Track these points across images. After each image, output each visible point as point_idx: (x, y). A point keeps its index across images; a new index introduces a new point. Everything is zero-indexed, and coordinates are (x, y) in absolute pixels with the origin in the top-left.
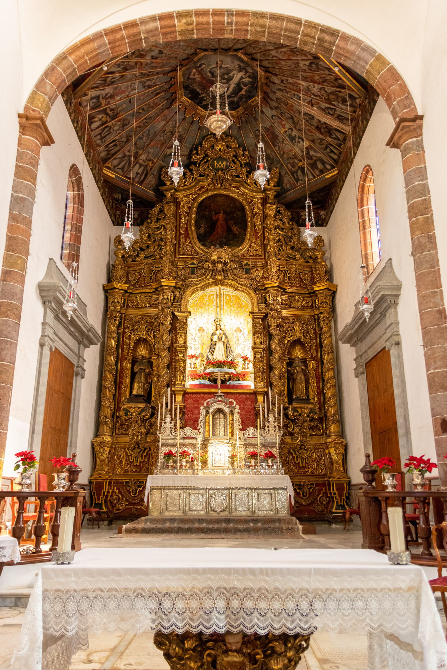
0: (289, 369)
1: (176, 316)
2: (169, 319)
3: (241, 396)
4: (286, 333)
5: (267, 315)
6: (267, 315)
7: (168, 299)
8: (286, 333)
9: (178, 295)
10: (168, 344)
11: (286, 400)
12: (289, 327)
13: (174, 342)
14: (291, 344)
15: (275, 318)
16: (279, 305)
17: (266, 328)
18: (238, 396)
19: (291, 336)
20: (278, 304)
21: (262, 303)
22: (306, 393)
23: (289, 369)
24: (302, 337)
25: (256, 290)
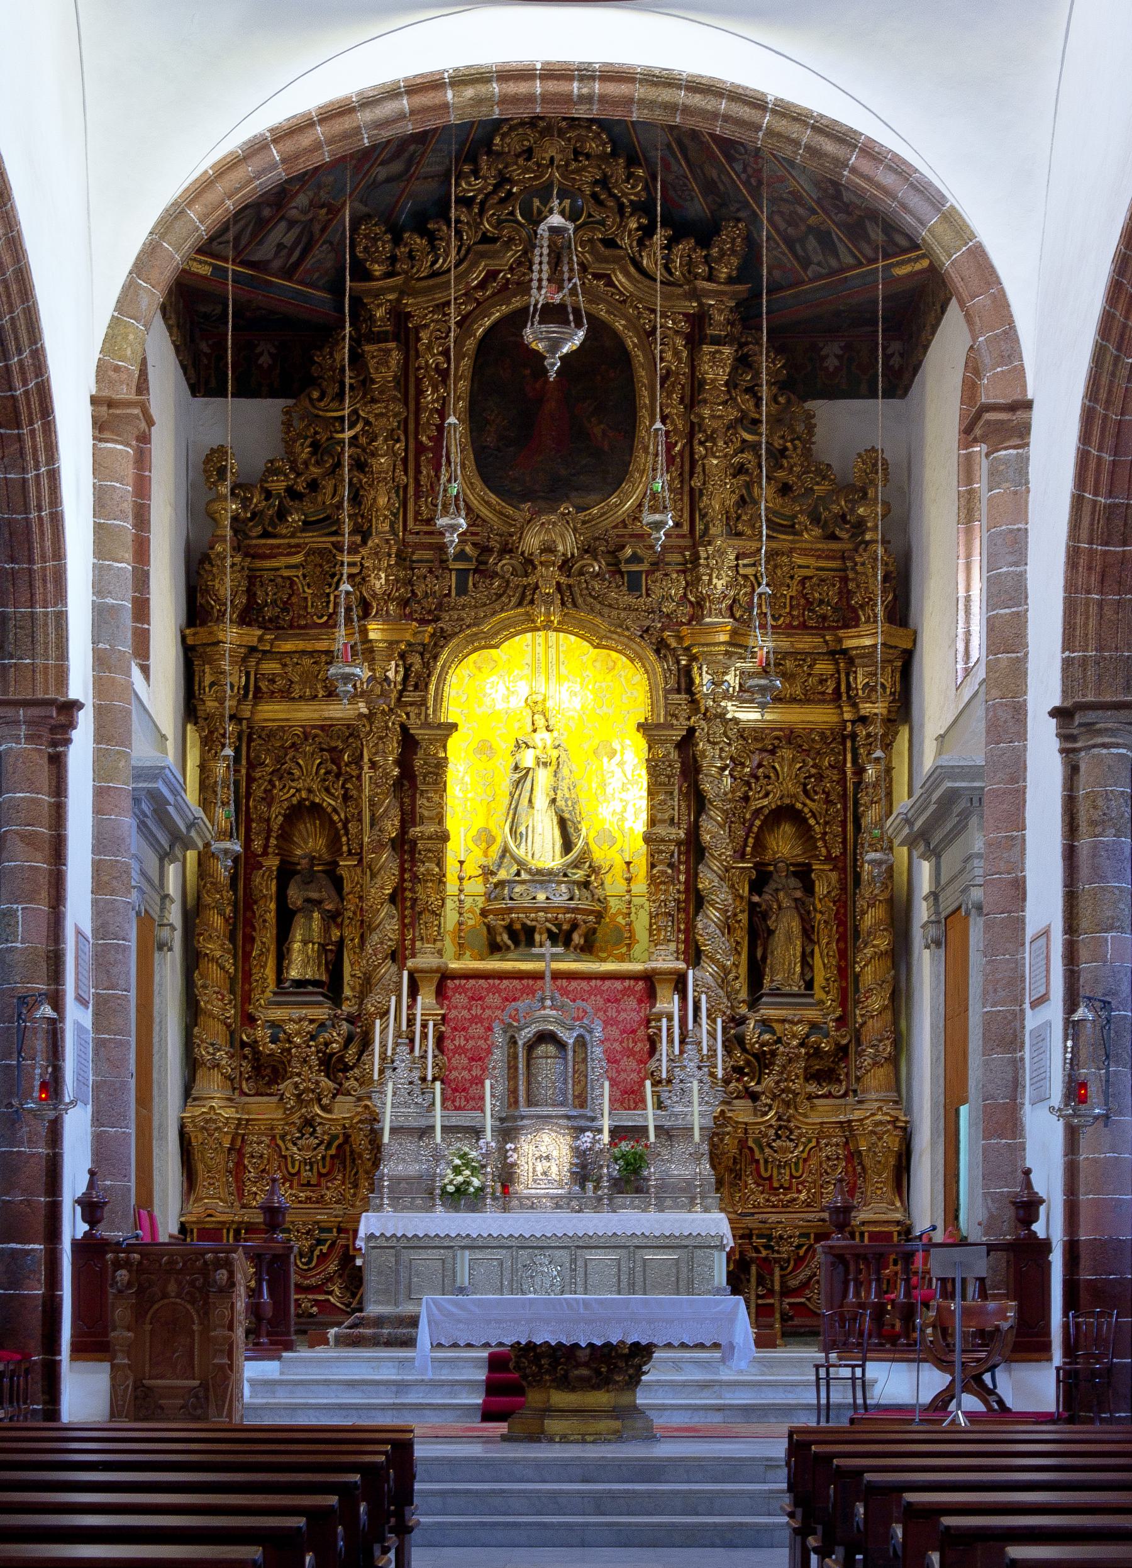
0: (756, 899)
1: (412, 736)
2: (393, 750)
3: (608, 983)
4: (748, 784)
5: (691, 731)
6: (691, 731)
7: (387, 679)
8: (748, 784)
9: (417, 667)
10: (391, 828)
11: (743, 995)
12: (760, 765)
13: (409, 818)
14: (764, 822)
15: (715, 743)
16: (730, 698)
17: (691, 769)
18: (599, 983)
19: (767, 795)
20: (727, 696)
21: (678, 691)
22: (802, 974)
23: (756, 899)
24: (802, 797)
25: (660, 647)
